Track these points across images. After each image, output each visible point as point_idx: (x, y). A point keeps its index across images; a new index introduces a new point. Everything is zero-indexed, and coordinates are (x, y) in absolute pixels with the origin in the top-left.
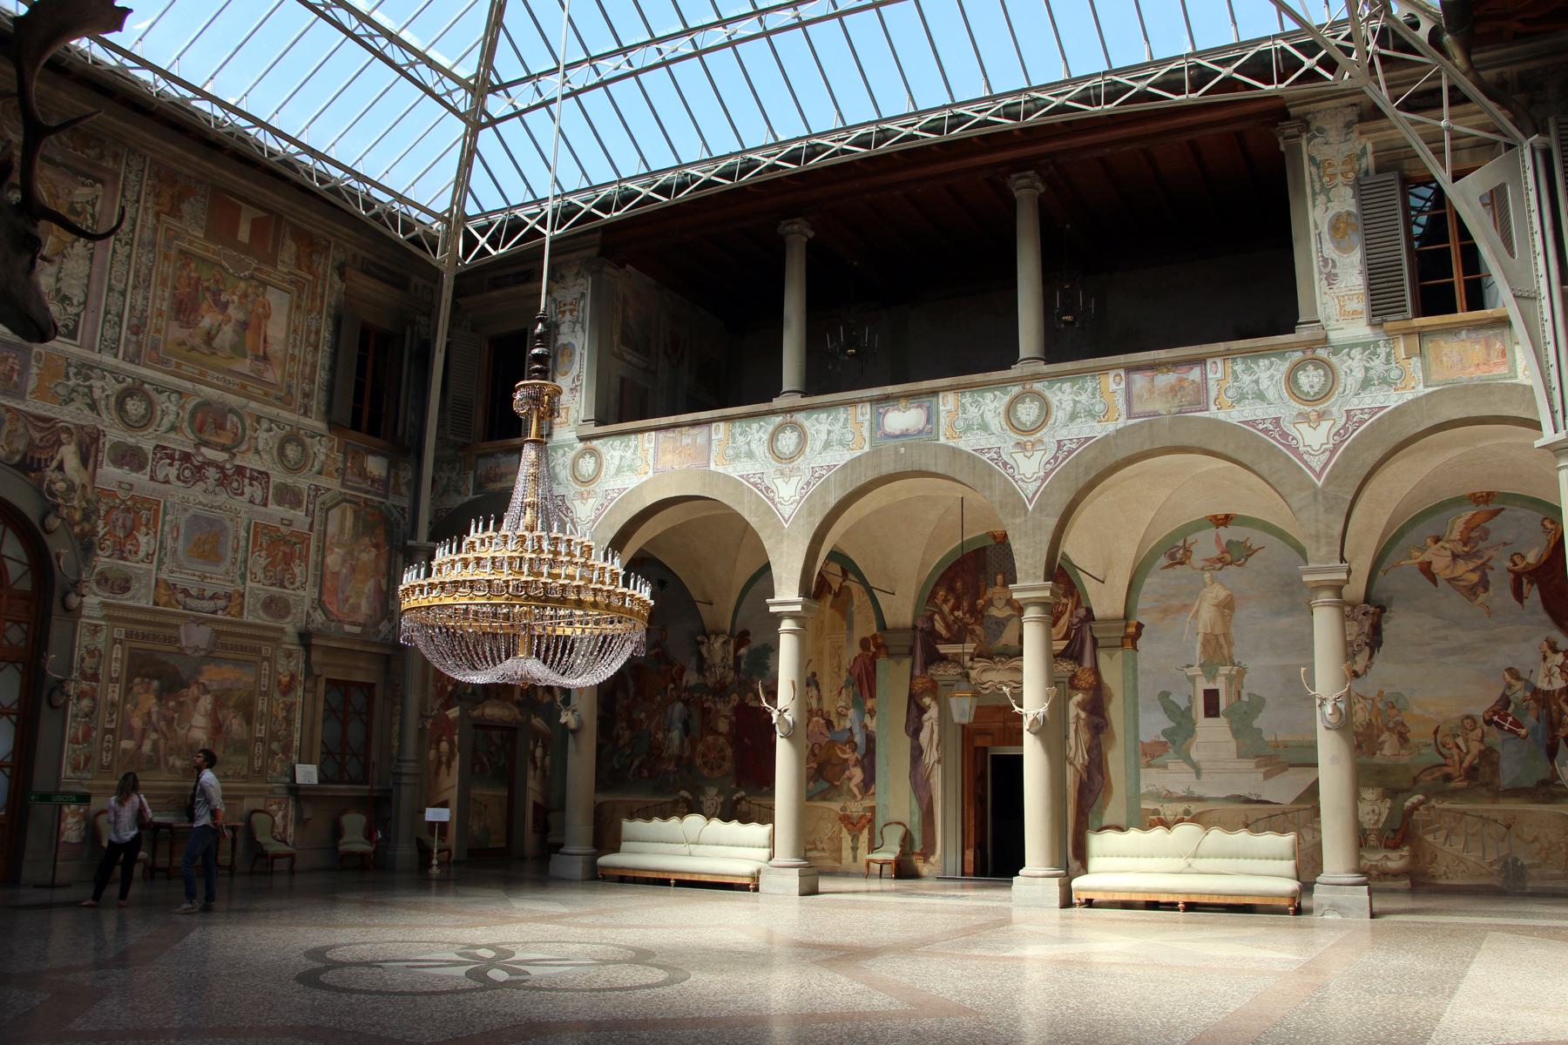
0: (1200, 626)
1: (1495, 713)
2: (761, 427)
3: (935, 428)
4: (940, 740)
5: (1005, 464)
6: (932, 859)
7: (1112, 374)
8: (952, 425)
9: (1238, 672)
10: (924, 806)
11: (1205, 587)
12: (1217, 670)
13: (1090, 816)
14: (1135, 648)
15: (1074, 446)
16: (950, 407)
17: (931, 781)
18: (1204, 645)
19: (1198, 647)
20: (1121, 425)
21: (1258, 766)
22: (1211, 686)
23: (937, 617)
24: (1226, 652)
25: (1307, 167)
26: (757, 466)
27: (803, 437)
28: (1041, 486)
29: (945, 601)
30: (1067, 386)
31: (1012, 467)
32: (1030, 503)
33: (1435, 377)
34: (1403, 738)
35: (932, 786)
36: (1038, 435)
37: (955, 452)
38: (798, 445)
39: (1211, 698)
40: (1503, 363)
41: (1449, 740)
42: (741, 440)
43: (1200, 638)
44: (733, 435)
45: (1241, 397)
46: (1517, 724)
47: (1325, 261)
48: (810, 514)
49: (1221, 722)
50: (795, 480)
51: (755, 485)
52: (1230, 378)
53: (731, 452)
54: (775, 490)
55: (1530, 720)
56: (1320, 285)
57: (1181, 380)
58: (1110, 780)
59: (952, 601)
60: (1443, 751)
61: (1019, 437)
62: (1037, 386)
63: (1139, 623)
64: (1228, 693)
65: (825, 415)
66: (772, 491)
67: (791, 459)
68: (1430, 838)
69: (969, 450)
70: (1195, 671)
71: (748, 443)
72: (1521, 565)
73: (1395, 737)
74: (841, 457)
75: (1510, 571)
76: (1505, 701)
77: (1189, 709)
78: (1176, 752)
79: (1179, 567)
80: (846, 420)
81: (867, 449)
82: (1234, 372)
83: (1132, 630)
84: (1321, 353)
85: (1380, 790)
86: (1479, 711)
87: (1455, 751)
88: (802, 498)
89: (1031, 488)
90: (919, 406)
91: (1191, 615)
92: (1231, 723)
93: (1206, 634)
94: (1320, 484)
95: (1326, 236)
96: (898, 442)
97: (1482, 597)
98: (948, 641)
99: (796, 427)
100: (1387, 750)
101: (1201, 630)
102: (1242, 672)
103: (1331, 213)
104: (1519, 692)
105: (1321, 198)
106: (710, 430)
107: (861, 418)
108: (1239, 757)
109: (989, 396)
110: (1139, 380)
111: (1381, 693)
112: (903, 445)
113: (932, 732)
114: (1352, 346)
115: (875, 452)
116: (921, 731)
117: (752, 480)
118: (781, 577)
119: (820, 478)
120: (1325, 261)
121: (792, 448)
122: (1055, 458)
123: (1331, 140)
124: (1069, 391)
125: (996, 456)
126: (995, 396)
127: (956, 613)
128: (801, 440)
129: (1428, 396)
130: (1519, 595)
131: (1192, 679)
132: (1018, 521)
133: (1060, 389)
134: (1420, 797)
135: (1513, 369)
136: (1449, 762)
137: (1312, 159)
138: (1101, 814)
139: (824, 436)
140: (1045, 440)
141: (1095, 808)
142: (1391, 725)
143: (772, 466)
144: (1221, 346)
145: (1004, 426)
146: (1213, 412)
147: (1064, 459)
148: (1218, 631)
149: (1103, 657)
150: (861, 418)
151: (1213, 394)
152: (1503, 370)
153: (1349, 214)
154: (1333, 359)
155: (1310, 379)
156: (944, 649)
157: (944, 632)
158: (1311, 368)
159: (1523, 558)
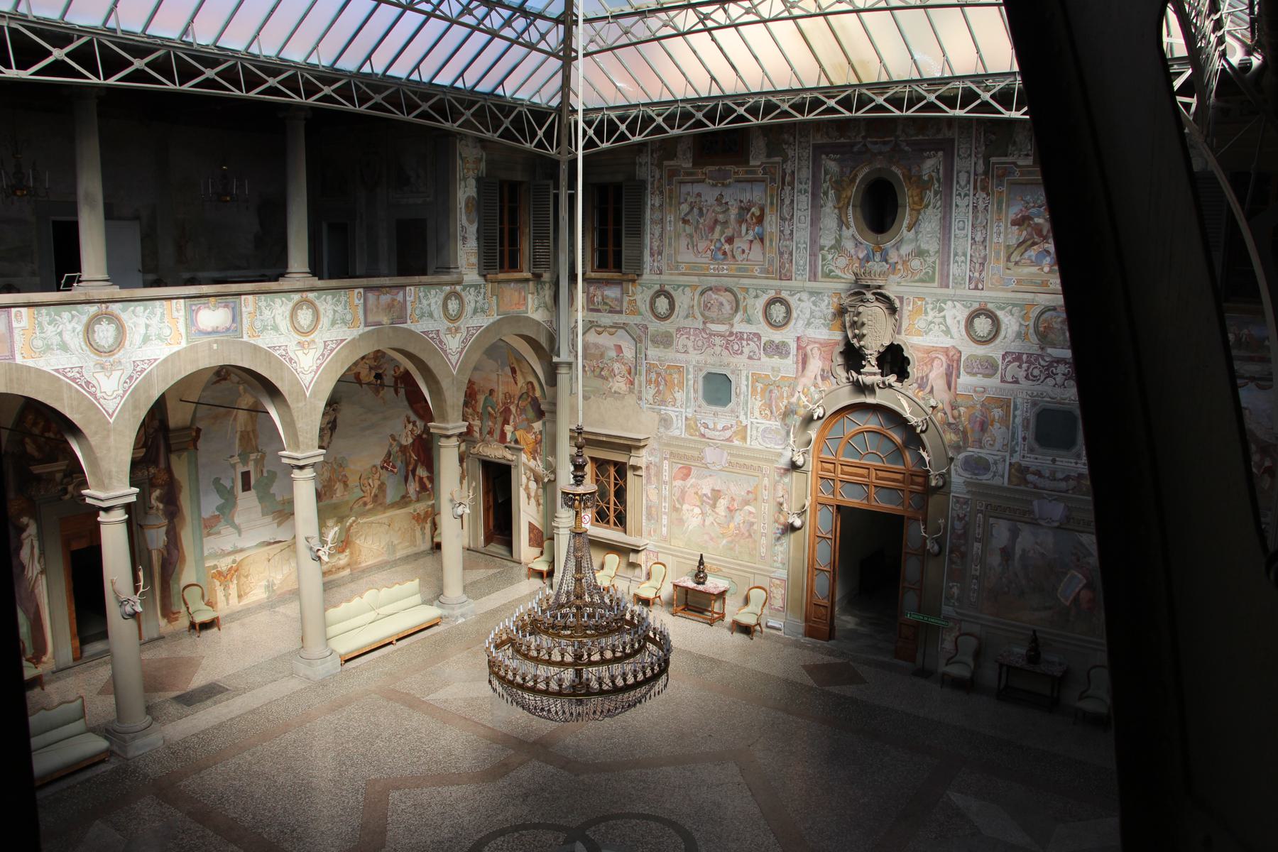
0: (238, 425)
1: (385, 462)
2: (73, 316)
3: (239, 327)
4: (42, 553)
5: (291, 359)
6: (44, 659)
7: (356, 291)
8: (252, 325)
9: (261, 456)
10: (32, 616)
11: (240, 395)
12: (249, 457)
13: (171, 582)
14: (196, 448)
15: (334, 346)
16: (251, 309)
17: (36, 591)
18: (240, 440)
19: (237, 441)
20: (361, 332)
21: (273, 520)
22: (246, 469)
23: (27, 440)
24: (254, 442)
25: (459, 162)
26: (74, 359)
27: (121, 330)
28: (313, 378)
29: (35, 424)
30: (329, 297)
31: (295, 362)
32: (307, 389)
33: (501, 310)
34: (346, 484)
35: (38, 596)
36: (312, 336)
37: (256, 348)
38: (116, 339)
39: (246, 475)
40: (524, 304)
41: (366, 482)
42: (50, 330)
43: (238, 435)
44: (40, 324)
45: (422, 316)
46: (394, 467)
47: (462, 227)
48: (136, 407)
49: (252, 493)
50: (116, 374)
51: (74, 380)
52: (417, 302)
53: (39, 343)
54: (96, 385)
55: (399, 464)
56: (460, 243)
57: (393, 300)
58: (183, 552)
59: (42, 423)
60: (363, 488)
61: (299, 337)
62: (311, 295)
63: (198, 428)
64: (256, 470)
65: (142, 308)
66: (94, 386)
67: (111, 352)
68: (358, 542)
69: (265, 347)
70: (236, 459)
71: (60, 334)
72: (398, 373)
73: (342, 485)
74: (160, 351)
75: (394, 377)
76: (389, 454)
77: (232, 488)
78: (225, 521)
79: (223, 382)
80: (163, 314)
81: (184, 344)
82: (419, 297)
83: (194, 434)
84: (458, 288)
85: (335, 519)
86: (378, 462)
87: (368, 487)
88: (125, 392)
89: (309, 378)
90: (226, 306)
91: (232, 419)
92: (257, 493)
93: (241, 432)
94: (455, 373)
95: (463, 211)
96: (211, 338)
97: (382, 393)
98: (40, 462)
99: (112, 318)
100: (338, 494)
101: (239, 429)
102: (263, 457)
103: (466, 196)
104: (395, 449)
105: (463, 183)
106: (9, 316)
107: (175, 314)
108: (263, 515)
109: (278, 301)
110: (371, 296)
111: (335, 458)
112: (216, 342)
113: (32, 547)
114: (471, 286)
115: (192, 348)
116: (21, 549)
117: (70, 375)
118: (110, 472)
119: (142, 371)
120: (462, 227)
121: (111, 341)
122: (323, 355)
123: (469, 144)
124: (330, 302)
125: (284, 353)
126: (282, 301)
127: (47, 435)
128: (119, 333)
129: (498, 320)
130: (397, 392)
131: (234, 466)
132: (301, 405)
133: (325, 300)
134: (353, 518)
135: (527, 308)
136: (366, 494)
137: (460, 154)
138: (179, 579)
139: (142, 330)
140: (316, 340)
141: (174, 575)
142: (340, 477)
143: (90, 361)
144: (417, 279)
145: (290, 329)
146: (409, 325)
147: (329, 355)
148: (249, 429)
149: (173, 458)
150: (175, 314)
151: (409, 312)
152: (523, 308)
153: (473, 198)
154: (463, 294)
155: (453, 305)
156: (38, 469)
157: (36, 454)
158: (453, 298)
159: (399, 369)
